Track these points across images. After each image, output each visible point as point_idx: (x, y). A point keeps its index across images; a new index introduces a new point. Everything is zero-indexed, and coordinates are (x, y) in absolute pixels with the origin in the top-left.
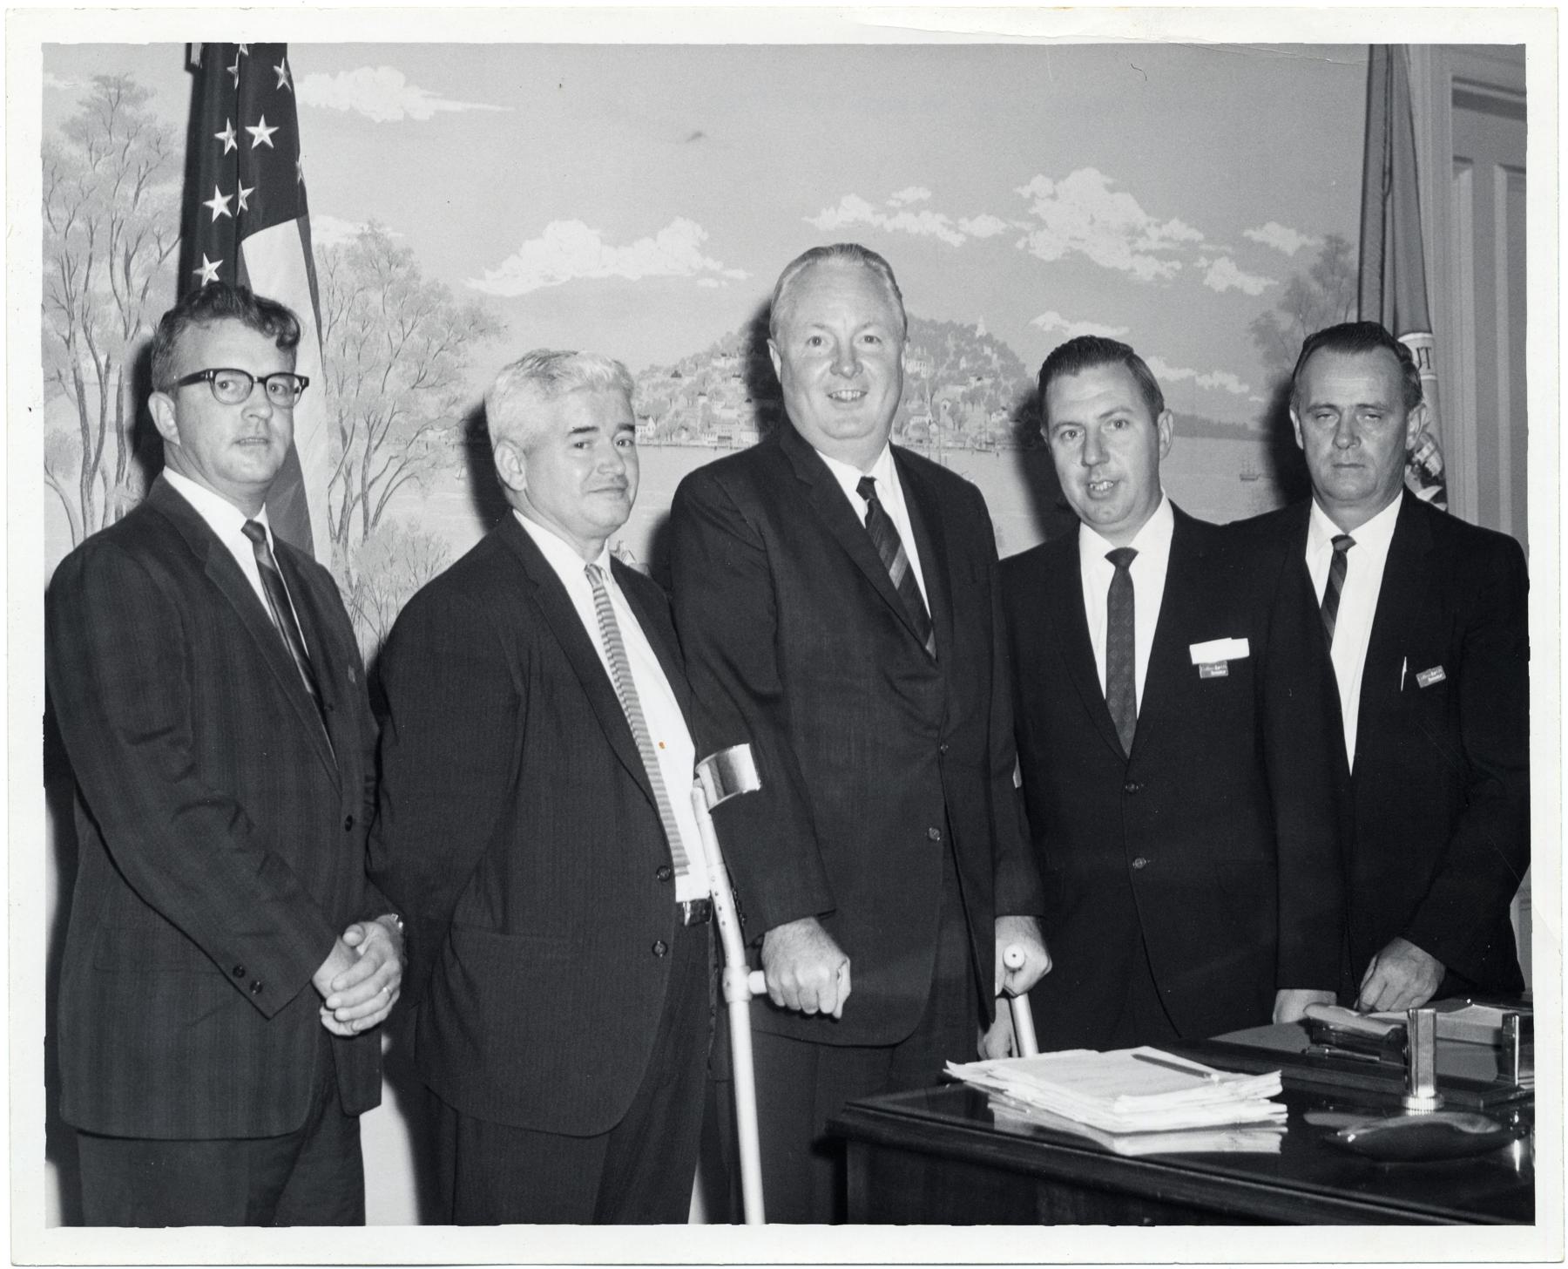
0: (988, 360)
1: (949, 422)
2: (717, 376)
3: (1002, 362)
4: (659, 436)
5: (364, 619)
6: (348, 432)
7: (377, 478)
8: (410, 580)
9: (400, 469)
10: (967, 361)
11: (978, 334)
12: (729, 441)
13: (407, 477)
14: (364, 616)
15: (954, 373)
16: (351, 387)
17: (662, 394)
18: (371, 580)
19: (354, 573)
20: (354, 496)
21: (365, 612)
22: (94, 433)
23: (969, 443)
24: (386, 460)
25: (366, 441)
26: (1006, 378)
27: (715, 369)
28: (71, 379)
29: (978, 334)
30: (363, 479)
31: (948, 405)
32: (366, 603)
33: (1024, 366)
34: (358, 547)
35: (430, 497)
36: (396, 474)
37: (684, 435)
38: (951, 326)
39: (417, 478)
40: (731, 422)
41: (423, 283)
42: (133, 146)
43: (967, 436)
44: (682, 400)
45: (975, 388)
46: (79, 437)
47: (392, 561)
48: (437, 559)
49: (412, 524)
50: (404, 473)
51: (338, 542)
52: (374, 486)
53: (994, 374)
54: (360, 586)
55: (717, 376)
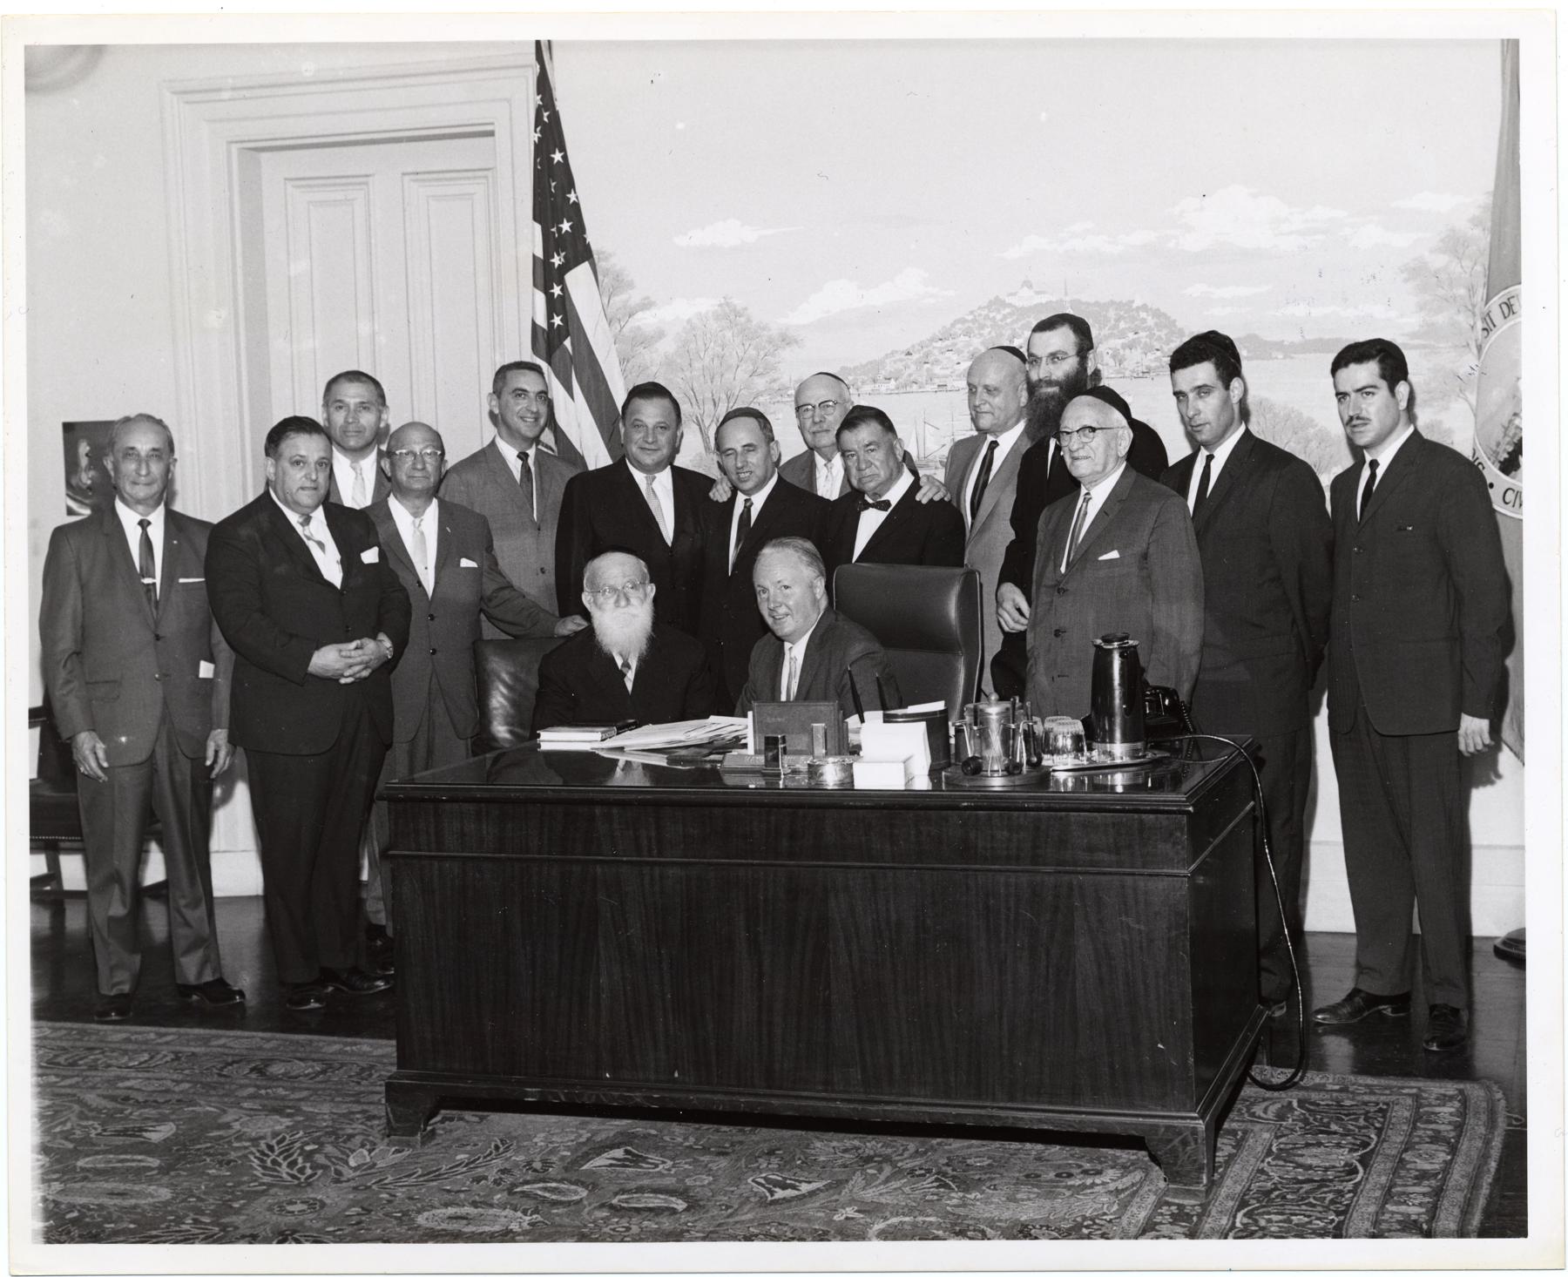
0: (1144, 321)
1: (1111, 362)
2: (936, 352)
3: (1156, 320)
4: (898, 388)
6: (717, 400)
10: (1126, 322)
11: (1134, 306)
12: (944, 388)
15: (1115, 332)
16: (717, 378)
17: (900, 366)
23: (1127, 373)
26: (1158, 331)
27: (934, 348)
29: (1134, 306)
31: (1110, 352)
33: (1175, 321)
37: (915, 385)
38: (1112, 303)
40: (946, 377)
41: (754, 323)
42: (606, 280)
43: (1126, 369)
44: (913, 367)
45: (1133, 340)
53: (1149, 329)
55: (936, 352)
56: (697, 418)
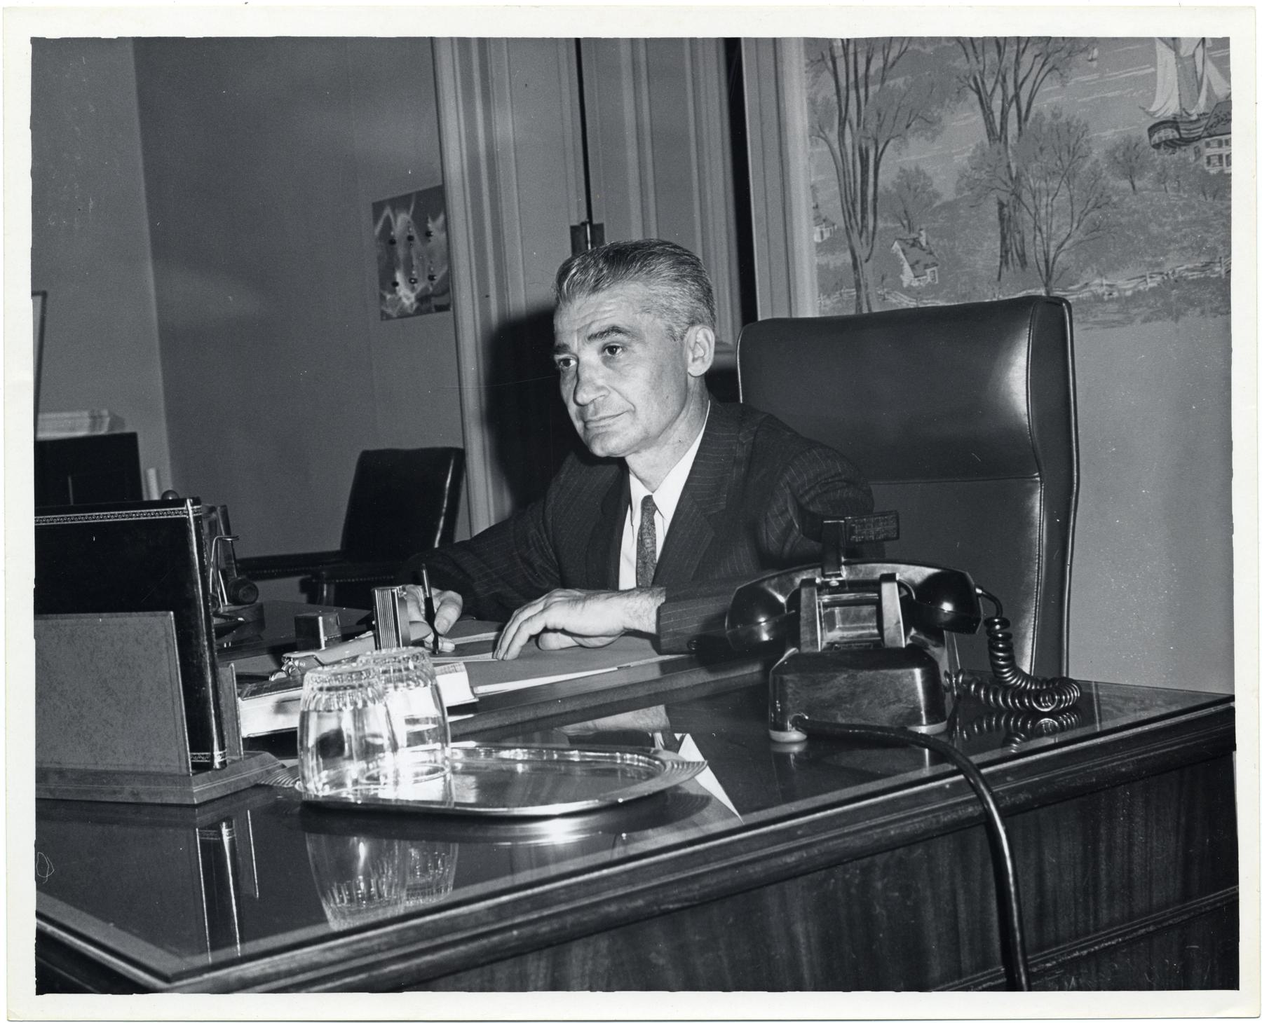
5: (1022, 206)
7: (1025, 78)
8: (1056, 165)
9: (1044, 65)
13: (1050, 71)
14: (1023, 204)
18: (1027, 170)
19: (1013, 165)
20: (1010, 98)
21: (1023, 199)
22: (843, 92)
24: (1032, 59)
25: (1015, 48)
28: (829, 58)
30: (1016, 81)
32: (1024, 190)
34: (1015, 142)
35: (1068, 84)
36: (1041, 69)
39: (1057, 69)
46: (835, 98)
47: (1041, 149)
48: (1077, 141)
49: (1056, 111)
50: (1046, 68)
51: (1000, 140)
52: (1024, 85)
54: (1016, 180)
56: (975, 79)
